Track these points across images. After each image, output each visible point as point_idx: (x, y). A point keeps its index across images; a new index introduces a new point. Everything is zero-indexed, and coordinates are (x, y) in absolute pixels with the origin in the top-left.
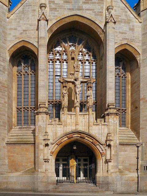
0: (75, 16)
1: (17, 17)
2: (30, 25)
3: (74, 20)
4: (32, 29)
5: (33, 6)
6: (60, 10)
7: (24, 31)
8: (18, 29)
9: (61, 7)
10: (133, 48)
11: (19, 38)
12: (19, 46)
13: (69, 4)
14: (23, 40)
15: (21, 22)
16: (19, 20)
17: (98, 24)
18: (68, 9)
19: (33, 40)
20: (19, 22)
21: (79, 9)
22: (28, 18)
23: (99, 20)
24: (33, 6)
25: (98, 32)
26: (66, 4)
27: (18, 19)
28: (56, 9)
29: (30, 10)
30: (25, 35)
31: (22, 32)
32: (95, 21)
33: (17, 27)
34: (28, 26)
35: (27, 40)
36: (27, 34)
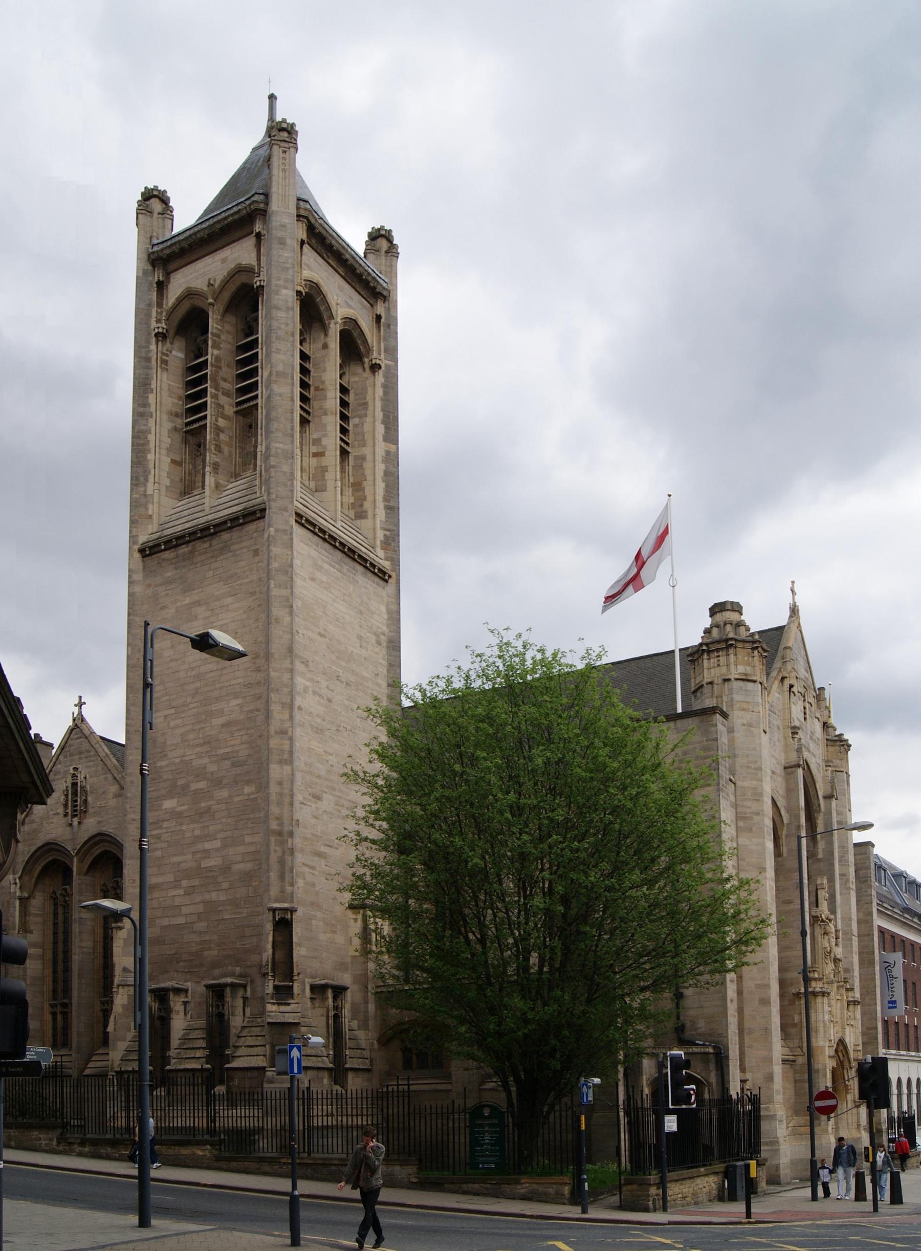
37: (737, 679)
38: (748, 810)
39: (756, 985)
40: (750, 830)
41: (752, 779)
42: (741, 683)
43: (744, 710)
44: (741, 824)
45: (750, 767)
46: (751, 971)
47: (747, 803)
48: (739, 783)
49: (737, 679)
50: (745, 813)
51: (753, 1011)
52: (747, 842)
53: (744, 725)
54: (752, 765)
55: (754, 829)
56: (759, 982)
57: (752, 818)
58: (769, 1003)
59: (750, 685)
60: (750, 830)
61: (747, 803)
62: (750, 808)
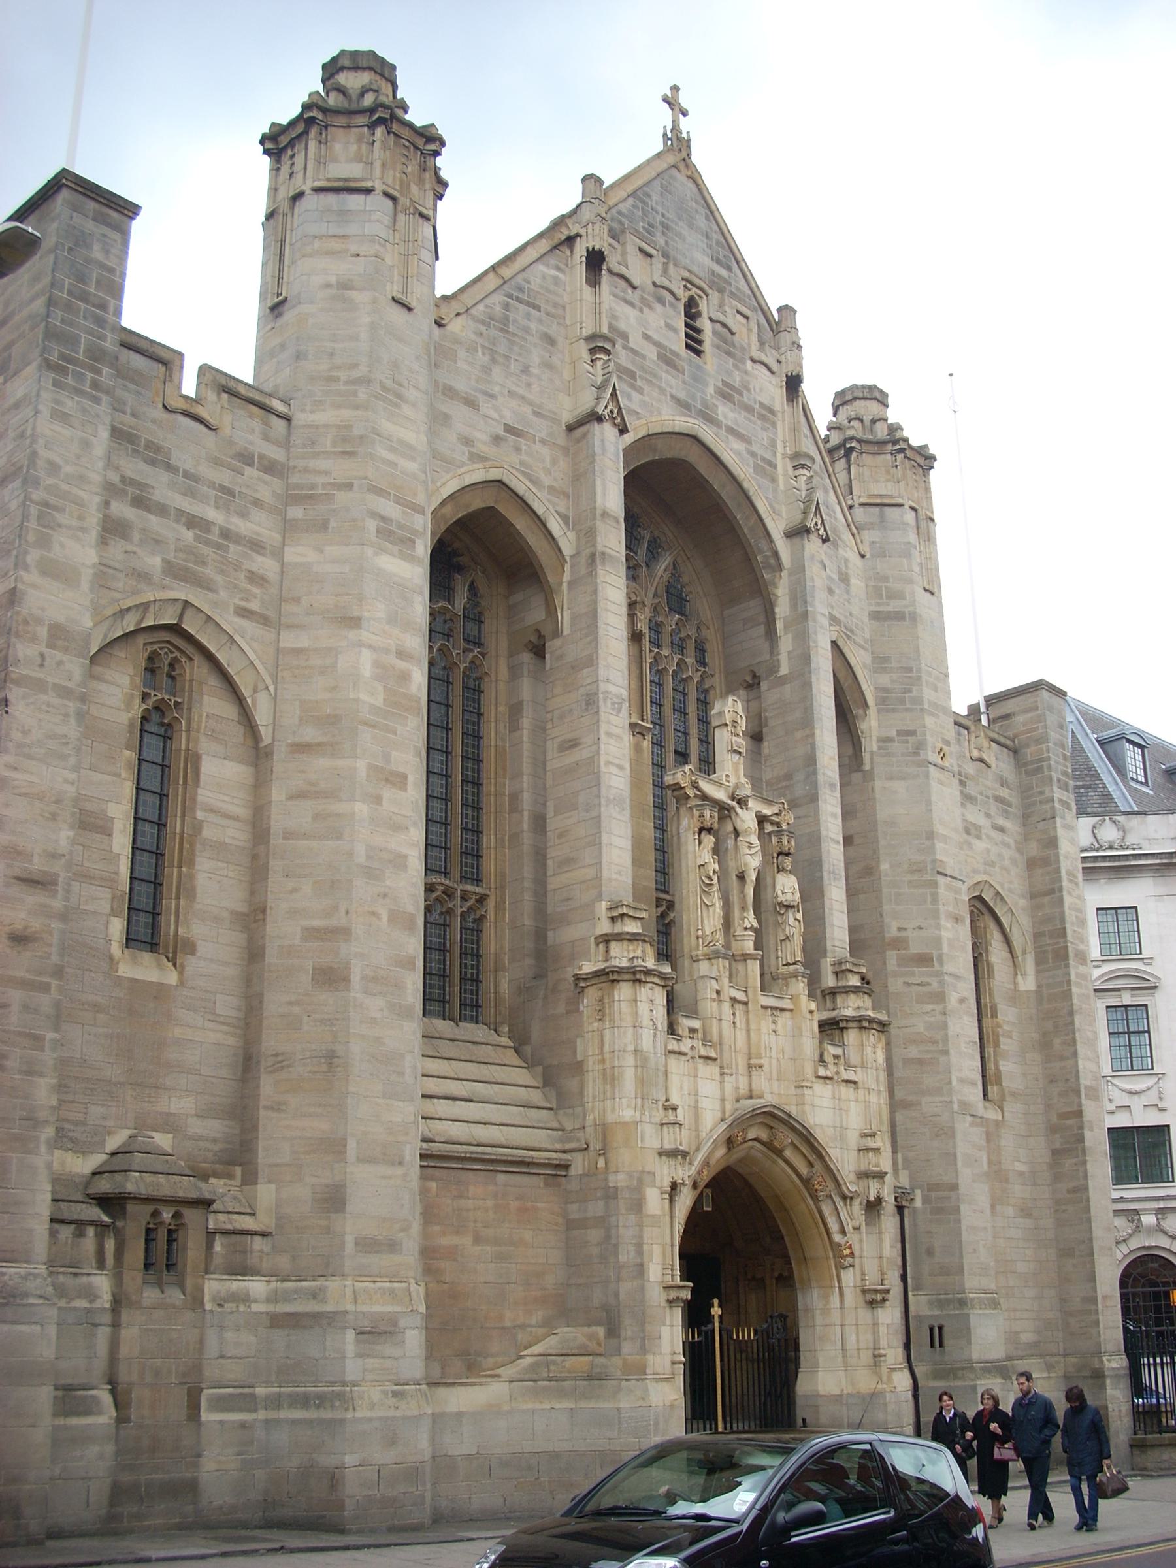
0: (689, 441)
1: (480, 340)
2: (536, 414)
3: (682, 455)
4: (543, 435)
5: (548, 314)
6: (647, 389)
7: (509, 429)
8: (486, 408)
9: (649, 377)
10: (851, 667)
11: (488, 464)
12: (477, 503)
13: (674, 372)
14: (500, 481)
15: (497, 373)
16: (487, 358)
17: (764, 516)
18: (672, 396)
19: (549, 500)
20: (486, 370)
21: (710, 419)
22: (526, 370)
23: (767, 498)
24: (548, 314)
25: (761, 551)
26: (665, 367)
27: (484, 354)
28: (633, 375)
29: (533, 326)
30: (515, 459)
31: (500, 431)
32: (753, 498)
33: (481, 398)
34: (527, 410)
35: (521, 489)
36: (524, 457)
37: (318, 190)
38: (321, 480)
39: (305, 929)
40: (324, 526)
41: (339, 407)
42: (331, 198)
43: (331, 253)
44: (295, 512)
45: (338, 379)
46: (295, 890)
47: (323, 464)
48: (300, 418)
49: (318, 190)
50: (313, 486)
51: (290, 1003)
52: (311, 556)
53: (328, 286)
54: (343, 375)
55: (332, 524)
56: (317, 923)
57: (329, 498)
58: (346, 980)
59: (355, 201)
60: (324, 526)
61: (323, 464)
62: (327, 473)
